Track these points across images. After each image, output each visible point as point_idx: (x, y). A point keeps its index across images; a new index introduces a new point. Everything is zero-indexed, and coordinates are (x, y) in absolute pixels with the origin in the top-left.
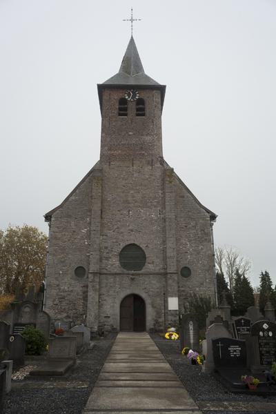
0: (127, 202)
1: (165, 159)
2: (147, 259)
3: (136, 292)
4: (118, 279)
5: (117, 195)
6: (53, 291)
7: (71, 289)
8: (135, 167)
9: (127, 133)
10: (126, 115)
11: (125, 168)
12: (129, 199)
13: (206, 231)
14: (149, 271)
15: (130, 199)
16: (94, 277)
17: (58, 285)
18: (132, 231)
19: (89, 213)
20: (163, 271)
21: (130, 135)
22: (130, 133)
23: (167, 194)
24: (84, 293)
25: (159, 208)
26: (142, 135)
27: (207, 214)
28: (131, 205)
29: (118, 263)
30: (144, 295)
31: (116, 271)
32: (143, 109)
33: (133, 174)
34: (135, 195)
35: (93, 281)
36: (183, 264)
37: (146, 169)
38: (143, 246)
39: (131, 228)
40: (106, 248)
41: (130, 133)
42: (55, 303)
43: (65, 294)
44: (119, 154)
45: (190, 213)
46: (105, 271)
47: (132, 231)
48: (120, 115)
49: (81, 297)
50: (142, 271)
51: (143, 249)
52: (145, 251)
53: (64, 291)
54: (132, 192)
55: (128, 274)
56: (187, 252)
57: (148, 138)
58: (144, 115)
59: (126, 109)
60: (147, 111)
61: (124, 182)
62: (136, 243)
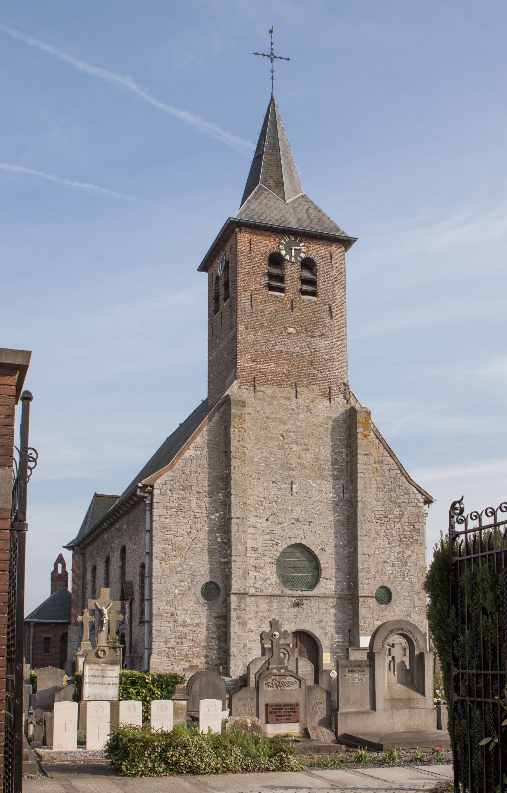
0: (288, 466)
1: (350, 387)
2: (323, 572)
3: (306, 627)
4: (275, 605)
5: (271, 453)
6: (166, 623)
7: (196, 621)
8: (300, 401)
9: (285, 328)
10: (282, 290)
11: (283, 401)
12: (291, 461)
13: (417, 526)
14: (324, 590)
15: (294, 461)
16: (240, 599)
17: (172, 615)
18: (297, 520)
19: (221, 485)
20: (347, 593)
21: (289, 334)
22: (291, 330)
23: (359, 457)
24: (219, 628)
25: (342, 482)
26: (312, 337)
27: (419, 496)
28: (295, 473)
29: (274, 578)
30: (317, 633)
31: (270, 591)
32: (313, 283)
33: (298, 414)
34: (303, 453)
35: (239, 607)
36: (383, 580)
37: (320, 406)
38: (316, 550)
39: (295, 515)
40: (254, 549)
41: (291, 330)
42: (170, 645)
43: (186, 630)
44: (272, 372)
45: (393, 494)
46: (252, 591)
47: (297, 520)
48: (271, 288)
49: (214, 636)
50: (315, 592)
51: (316, 552)
52: (319, 557)
53: (184, 624)
54: (296, 448)
55: (293, 596)
56: (385, 562)
57: (322, 344)
58: (314, 294)
59: (281, 278)
60: (321, 286)
61: (281, 427)
62: (304, 542)
